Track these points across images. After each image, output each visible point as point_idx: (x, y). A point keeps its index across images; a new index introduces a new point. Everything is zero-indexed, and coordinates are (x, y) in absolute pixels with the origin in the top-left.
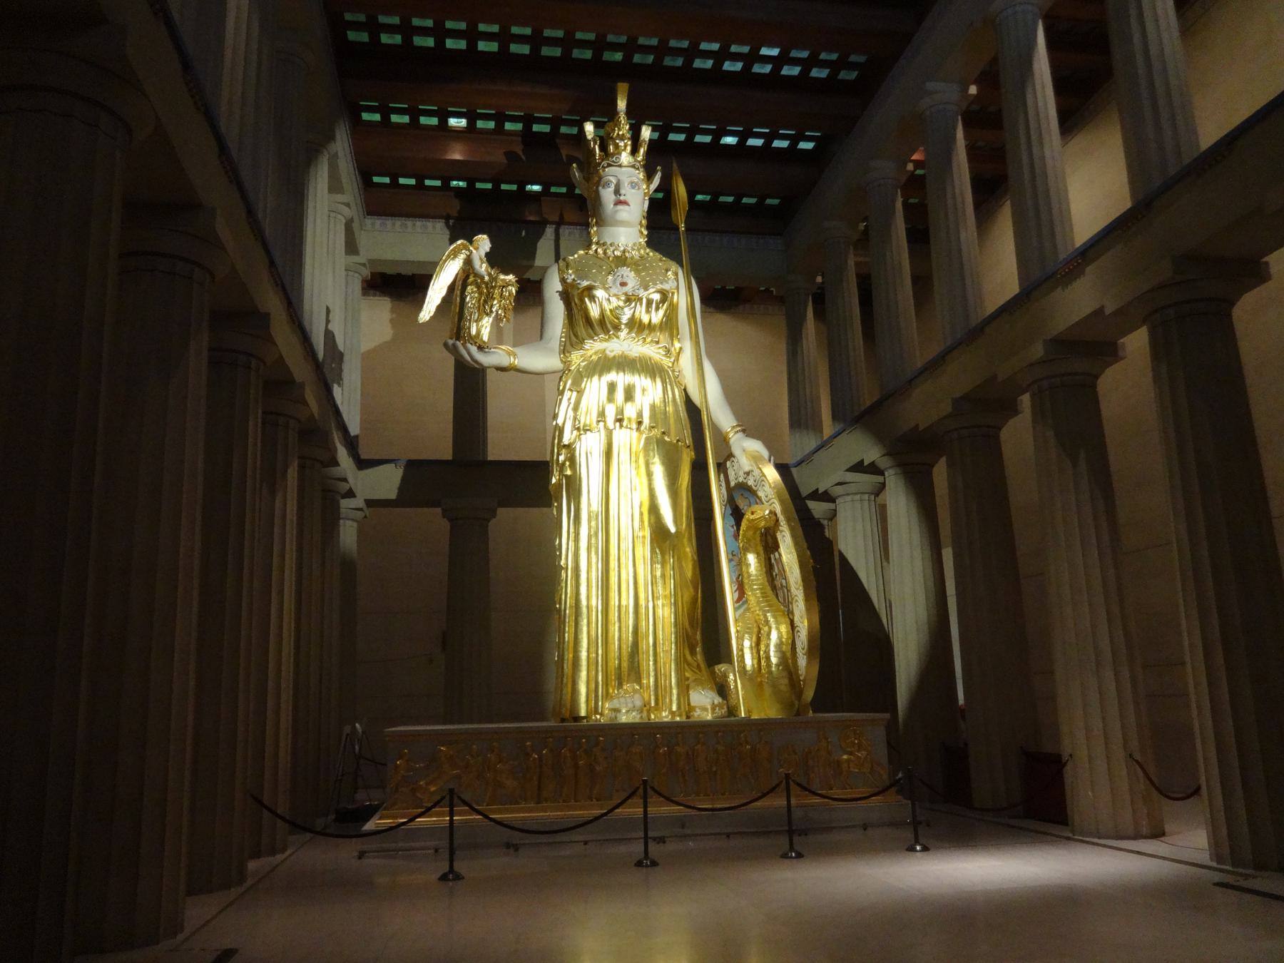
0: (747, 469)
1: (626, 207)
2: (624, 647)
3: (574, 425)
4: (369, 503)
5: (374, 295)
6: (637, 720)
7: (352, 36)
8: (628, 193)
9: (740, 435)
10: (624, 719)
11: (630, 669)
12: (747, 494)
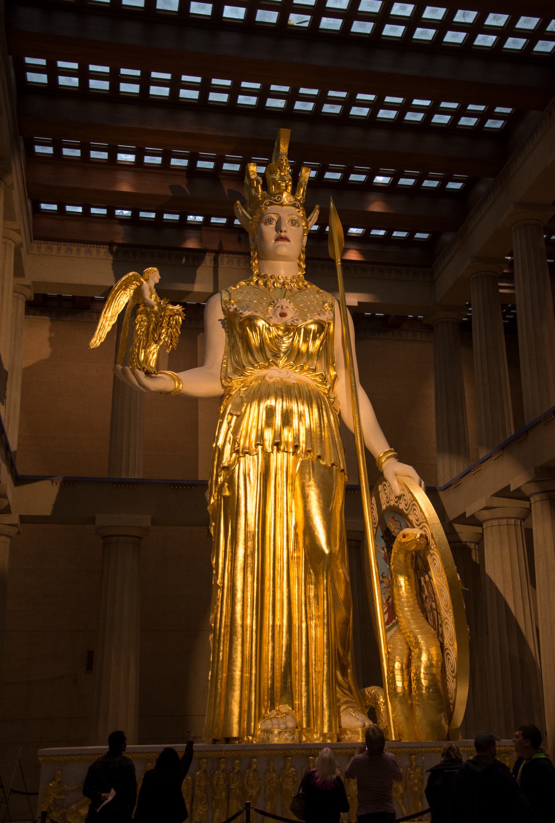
0: (398, 492)
1: (287, 243)
2: (277, 667)
3: (233, 448)
4: (24, 519)
5: (35, 314)
6: (289, 742)
7: (32, 77)
8: (291, 231)
9: (393, 461)
10: (276, 740)
11: (283, 689)
12: (397, 517)
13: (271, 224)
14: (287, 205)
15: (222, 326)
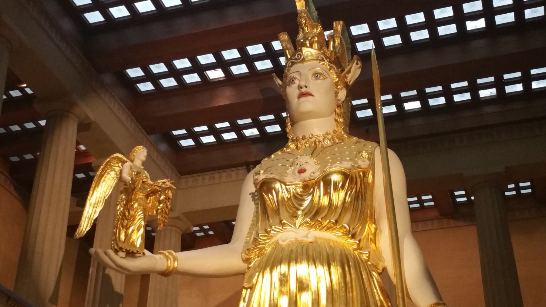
1: (310, 98)
8: (314, 86)
13: (294, 83)
14: (310, 60)
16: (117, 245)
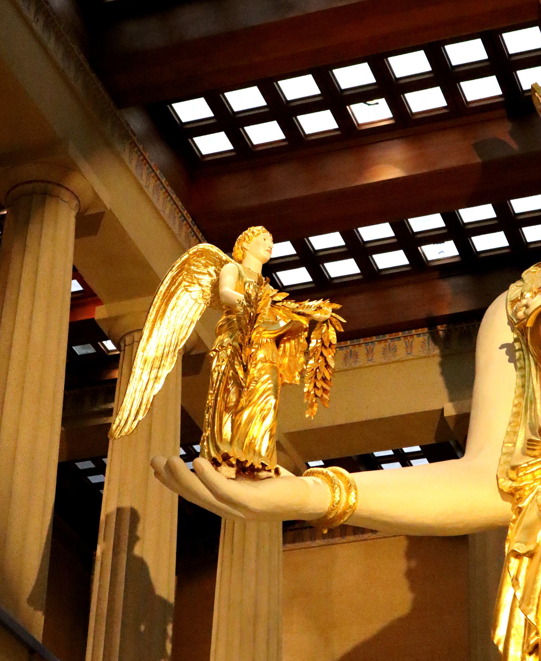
15: (508, 357)
16: (217, 449)
